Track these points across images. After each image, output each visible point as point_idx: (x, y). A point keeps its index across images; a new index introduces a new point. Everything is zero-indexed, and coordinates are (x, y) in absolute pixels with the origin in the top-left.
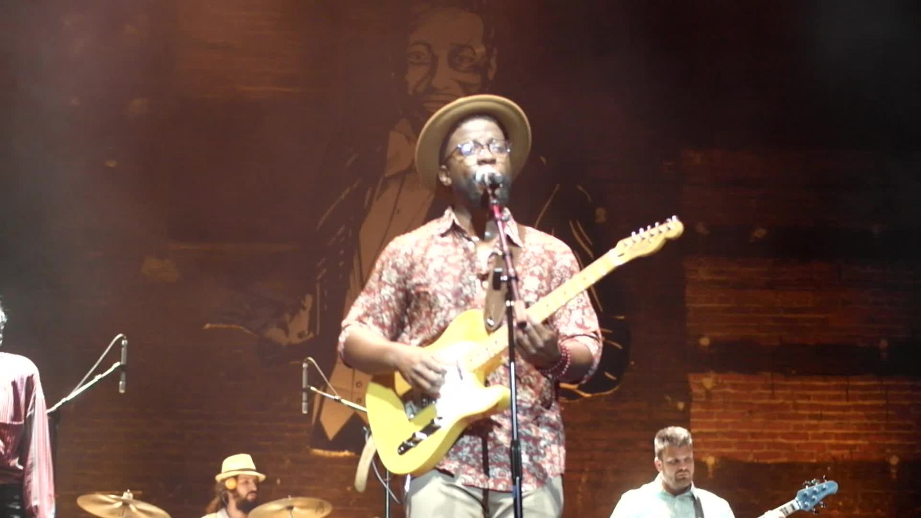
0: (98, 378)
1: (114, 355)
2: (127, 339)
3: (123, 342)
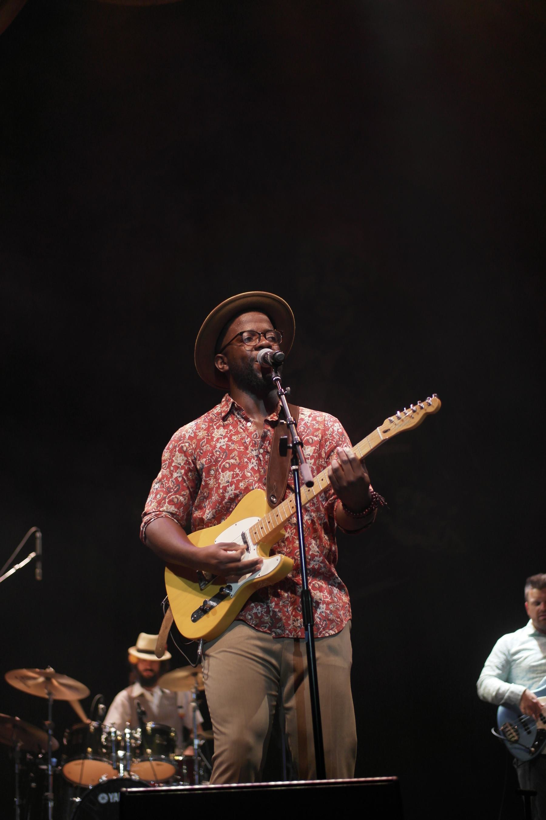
0: (17, 567)
2: (42, 532)
3: (39, 535)
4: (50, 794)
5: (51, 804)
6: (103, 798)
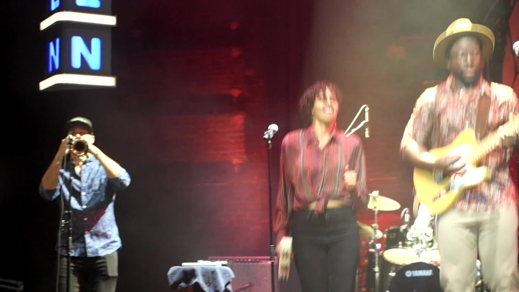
1: (362, 117)
4: (377, 269)
5: (377, 275)
6: (408, 274)
